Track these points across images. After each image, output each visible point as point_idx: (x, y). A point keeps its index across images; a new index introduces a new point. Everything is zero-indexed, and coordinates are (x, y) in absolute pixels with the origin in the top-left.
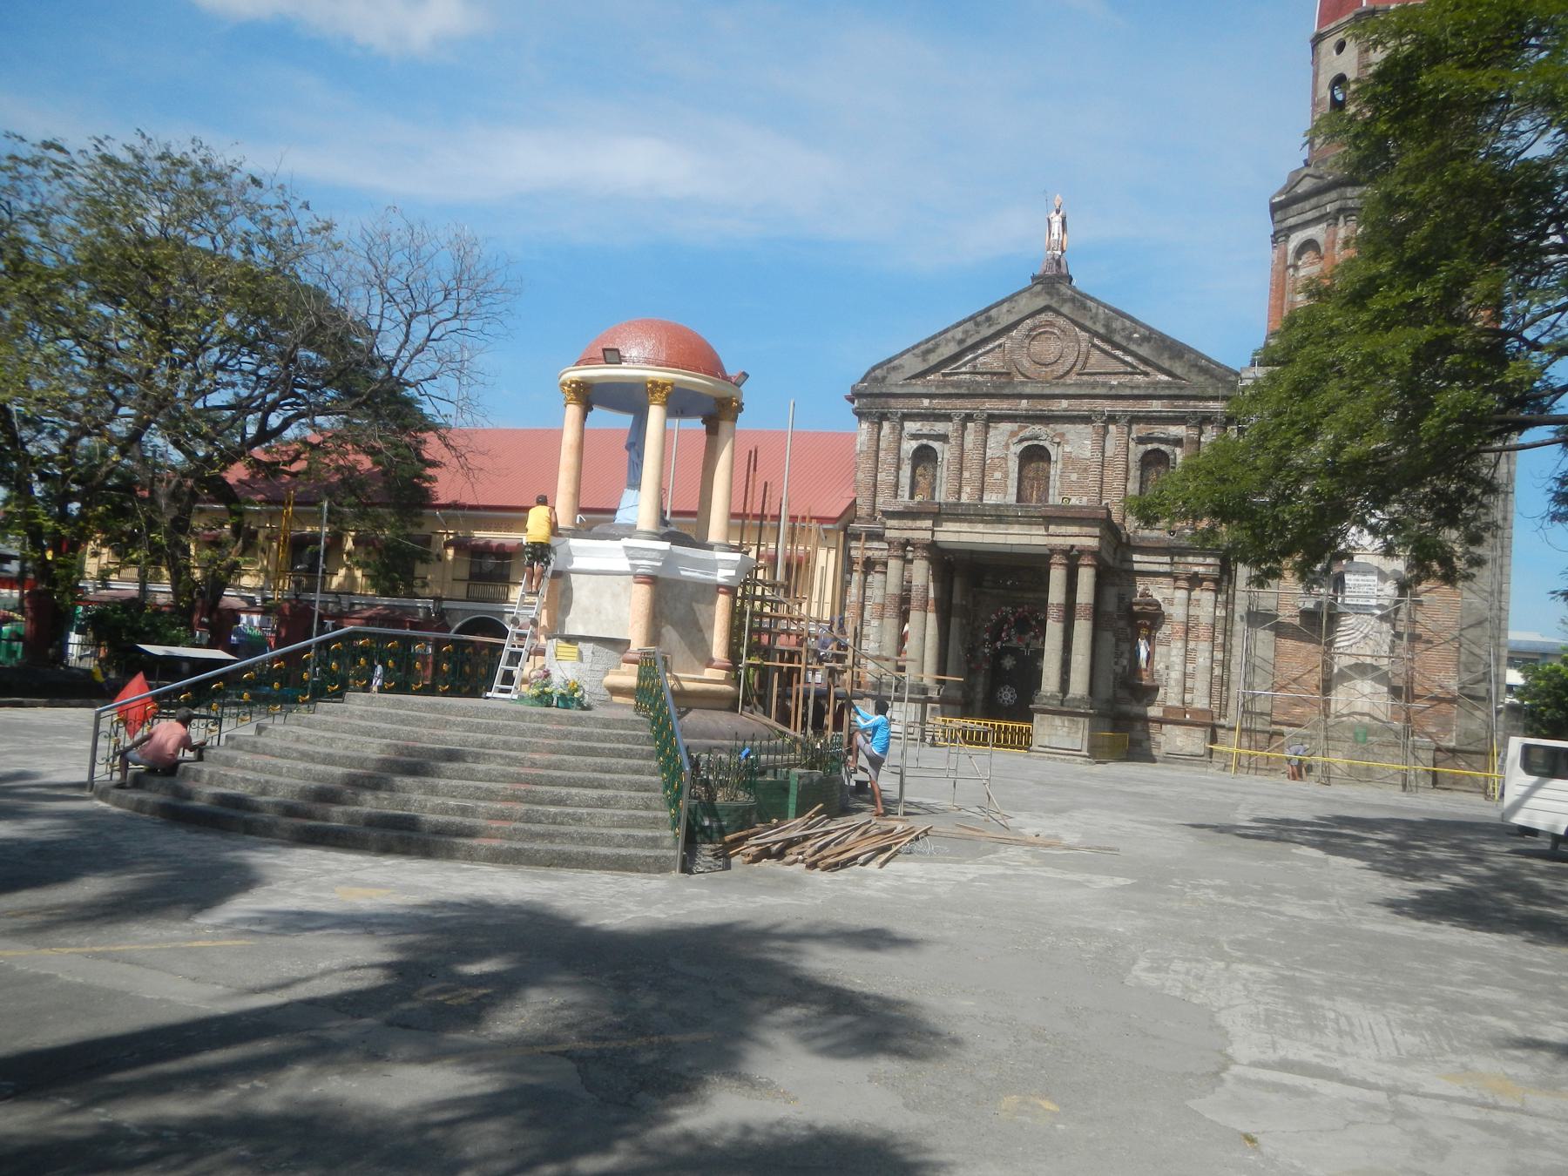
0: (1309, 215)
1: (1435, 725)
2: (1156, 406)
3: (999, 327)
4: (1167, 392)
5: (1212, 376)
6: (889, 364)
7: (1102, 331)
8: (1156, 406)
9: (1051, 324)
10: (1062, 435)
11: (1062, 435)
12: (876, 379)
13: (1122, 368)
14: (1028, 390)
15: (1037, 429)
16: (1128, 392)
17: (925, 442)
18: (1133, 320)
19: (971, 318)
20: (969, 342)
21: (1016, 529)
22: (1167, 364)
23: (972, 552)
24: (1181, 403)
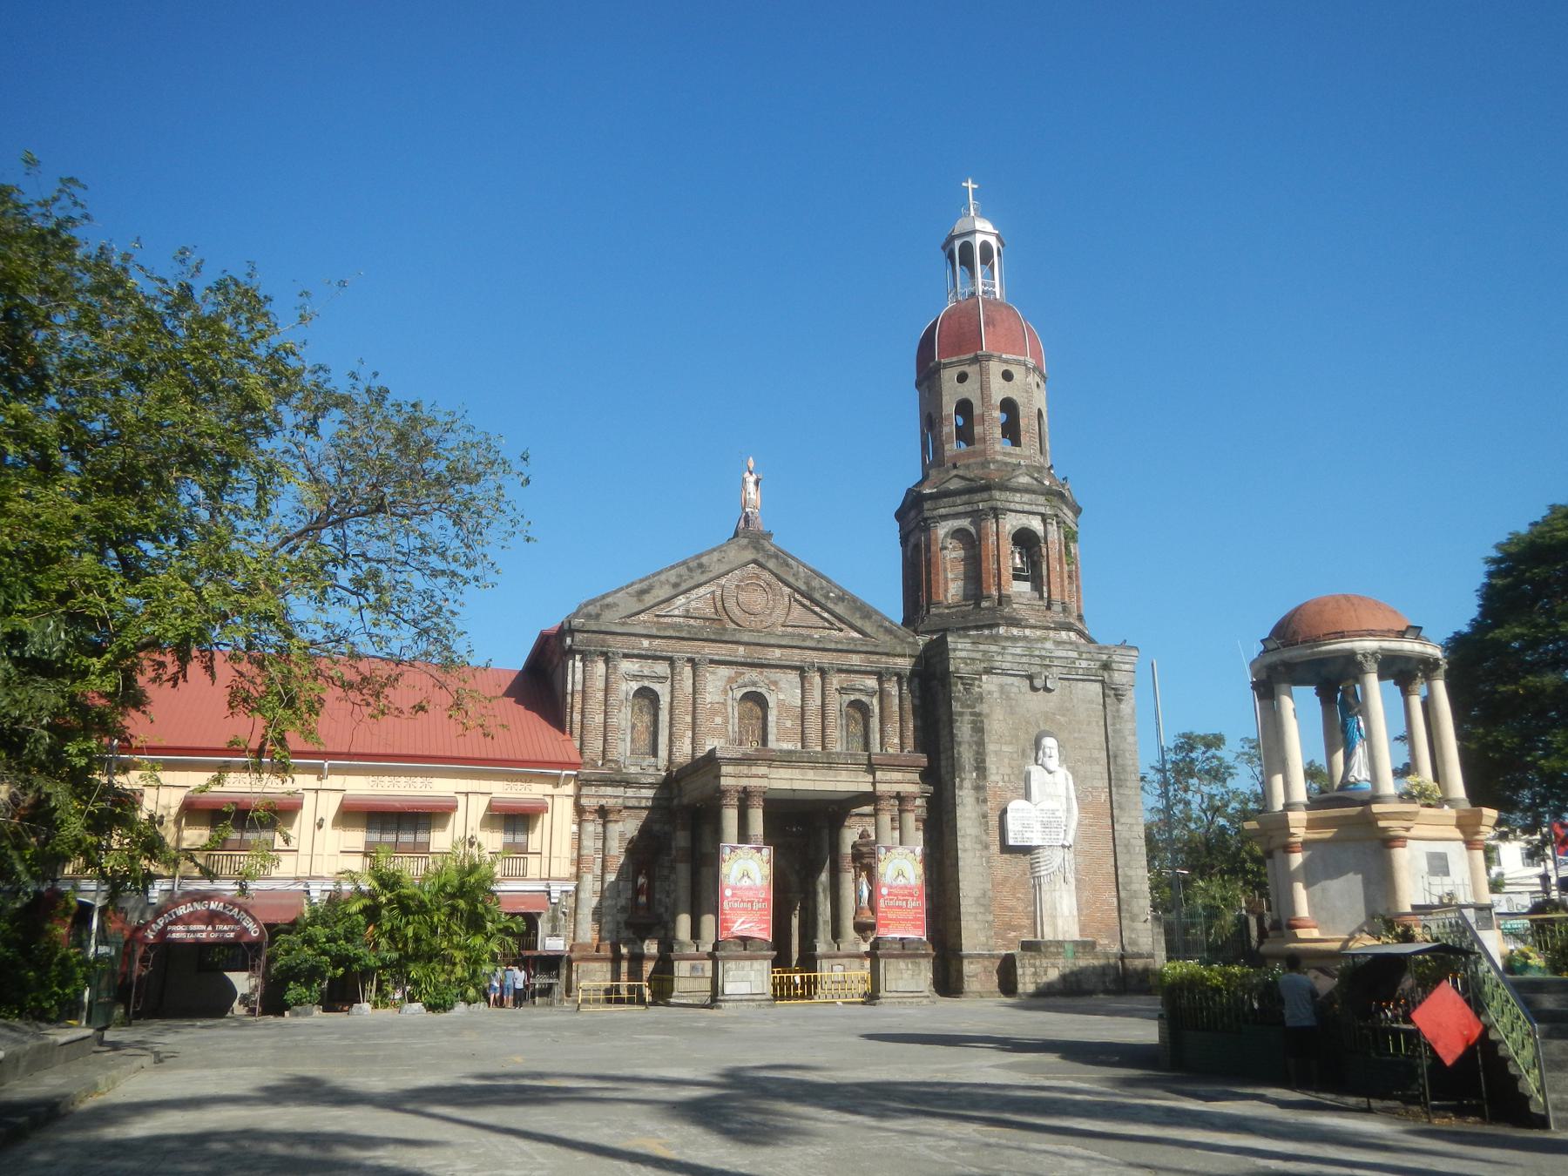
0: (961, 509)
2: (856, 660)
3: (711, 575)
4: (865, 648)
5: (896, 637)
6: (602, 603)
7: (803, 588)
8: (856, 660)
9: (758, 577)
10: (775, 683)
11: (775, 683)
12: (589, 616)
13: (821, 623)
14: (745, 638)
15: (752, 675)
16: (833, 646)
17: (646, 683)
18: (829, 581)
19: (684, 563)
20: (684, 587)
21: (844, 776)
22: (859, 623)
24: (874, 658)
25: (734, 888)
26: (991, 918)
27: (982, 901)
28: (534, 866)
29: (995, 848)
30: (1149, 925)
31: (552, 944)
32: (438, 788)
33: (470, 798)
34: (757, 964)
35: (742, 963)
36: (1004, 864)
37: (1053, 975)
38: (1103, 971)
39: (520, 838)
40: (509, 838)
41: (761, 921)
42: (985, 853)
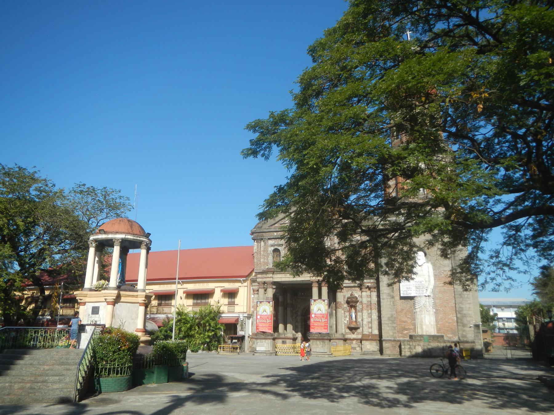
1: (451, 334)
12: (259, 227)
17: (276, 247)
23: (292, 284)
25: (261, 315)
26: (395, 325)
27: (391, 319)
28: (237, 309)
29: (398, 298)
30: (472, 329)
31: (240, 333)
32: (210, 286)
33: (218, 287)
34: (267, 341)
35: (262, 340)
36: (401, 304)
37: (419, 349)
38: (443, 349)
39: (233, 300)
40: (230, 300)
41: (269, 326)
42: (392, 300)
